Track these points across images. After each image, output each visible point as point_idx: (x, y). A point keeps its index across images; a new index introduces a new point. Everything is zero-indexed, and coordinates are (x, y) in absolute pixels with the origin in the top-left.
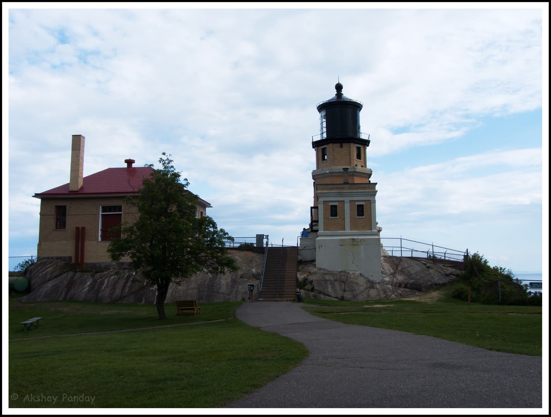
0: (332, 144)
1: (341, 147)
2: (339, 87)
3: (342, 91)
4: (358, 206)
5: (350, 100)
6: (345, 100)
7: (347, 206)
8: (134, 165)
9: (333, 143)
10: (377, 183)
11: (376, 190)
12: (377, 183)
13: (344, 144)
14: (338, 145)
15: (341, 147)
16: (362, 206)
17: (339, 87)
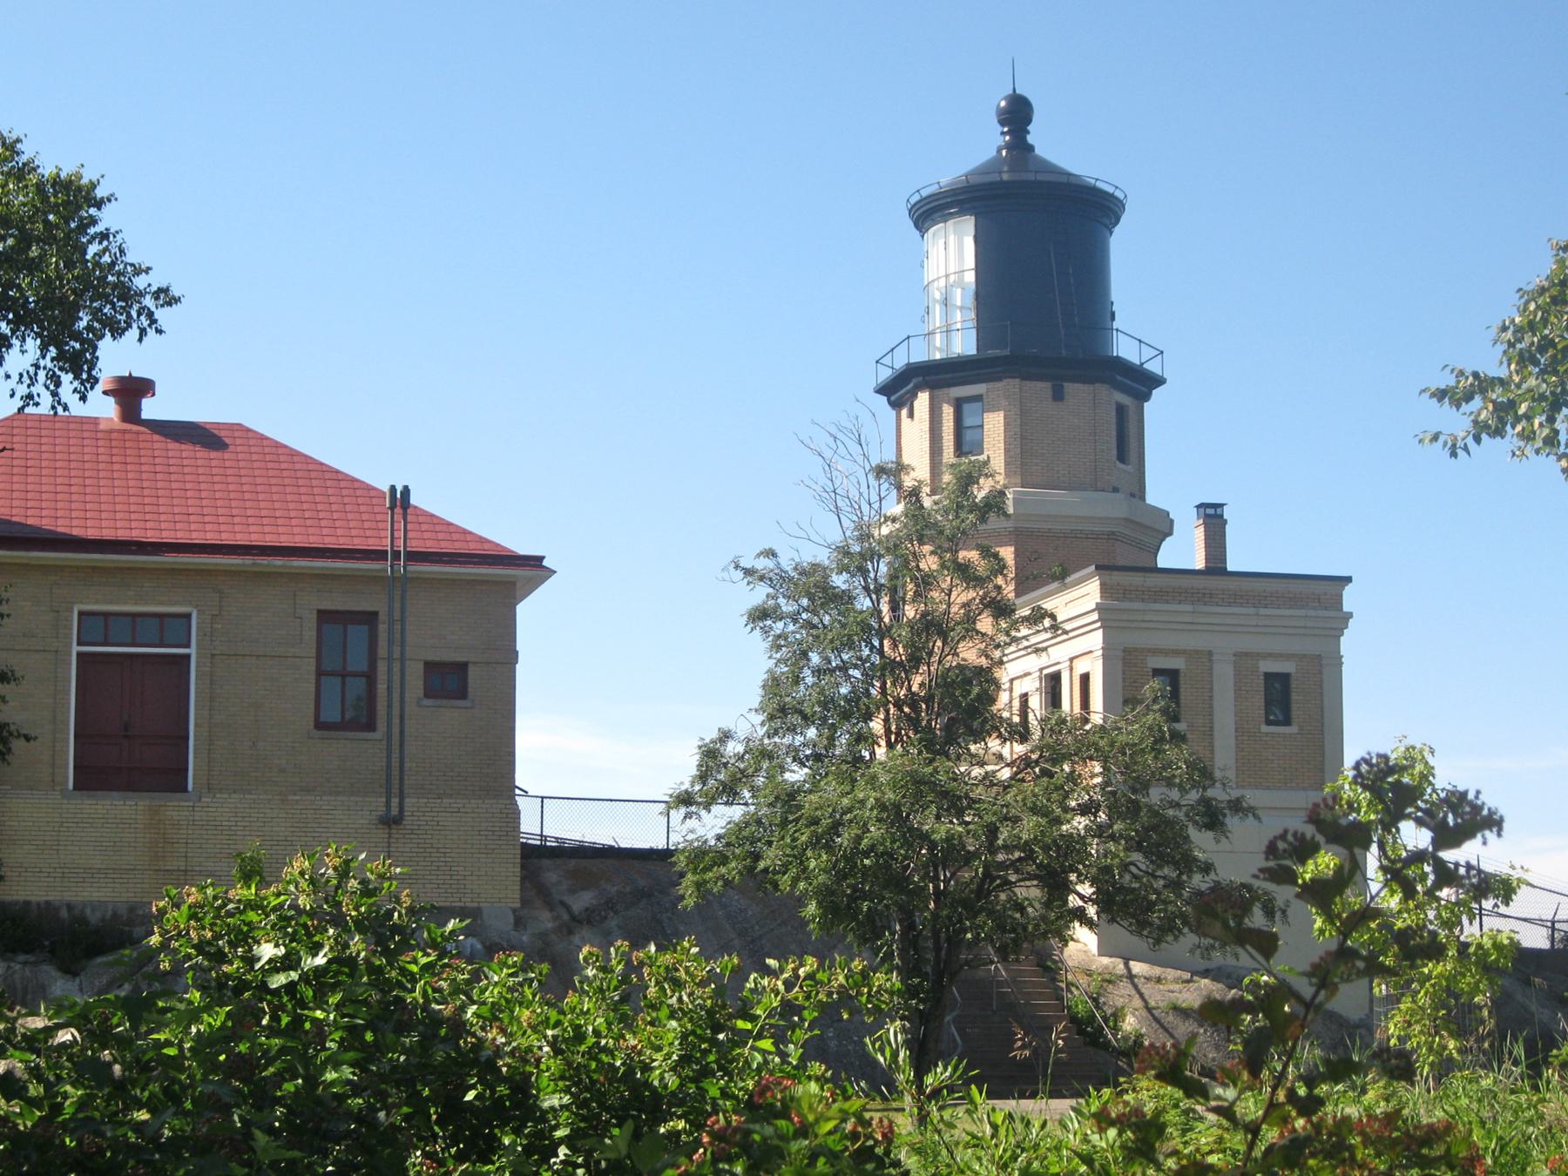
0: (1018, 380)
1: (1058, 396)
2: (1017, 114)
3: (1028, 132)
4: (1269, 677)
5: (1064, 179)
6: (1041, 177)
7: (1224, 677)
8: (151, 409)
9: (1026, 377)
10: (1349, 580)
11: (1346, 609)
12: (1349, 580)
13: (1069, 387)
14: (1044, 388)
15: (1058, 396)
16: (1284, 678)
17: (1017, 114)
